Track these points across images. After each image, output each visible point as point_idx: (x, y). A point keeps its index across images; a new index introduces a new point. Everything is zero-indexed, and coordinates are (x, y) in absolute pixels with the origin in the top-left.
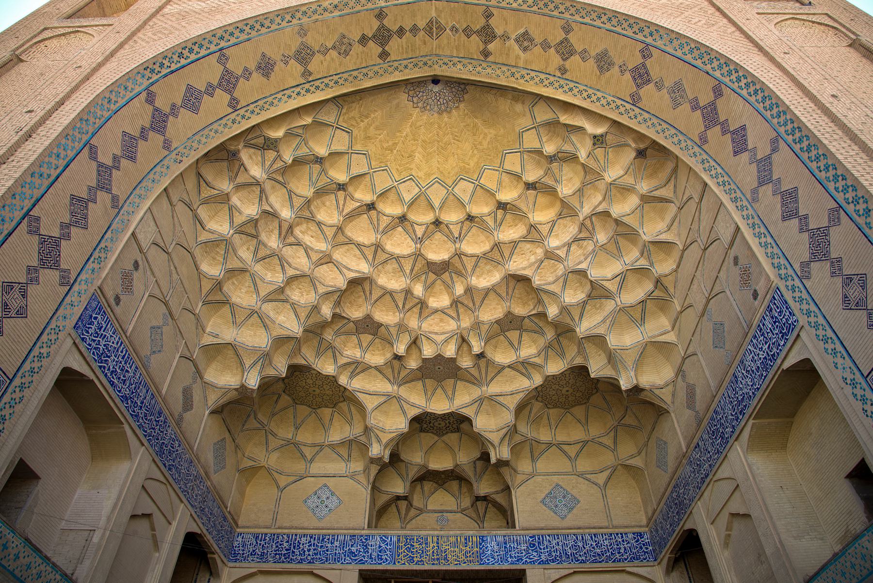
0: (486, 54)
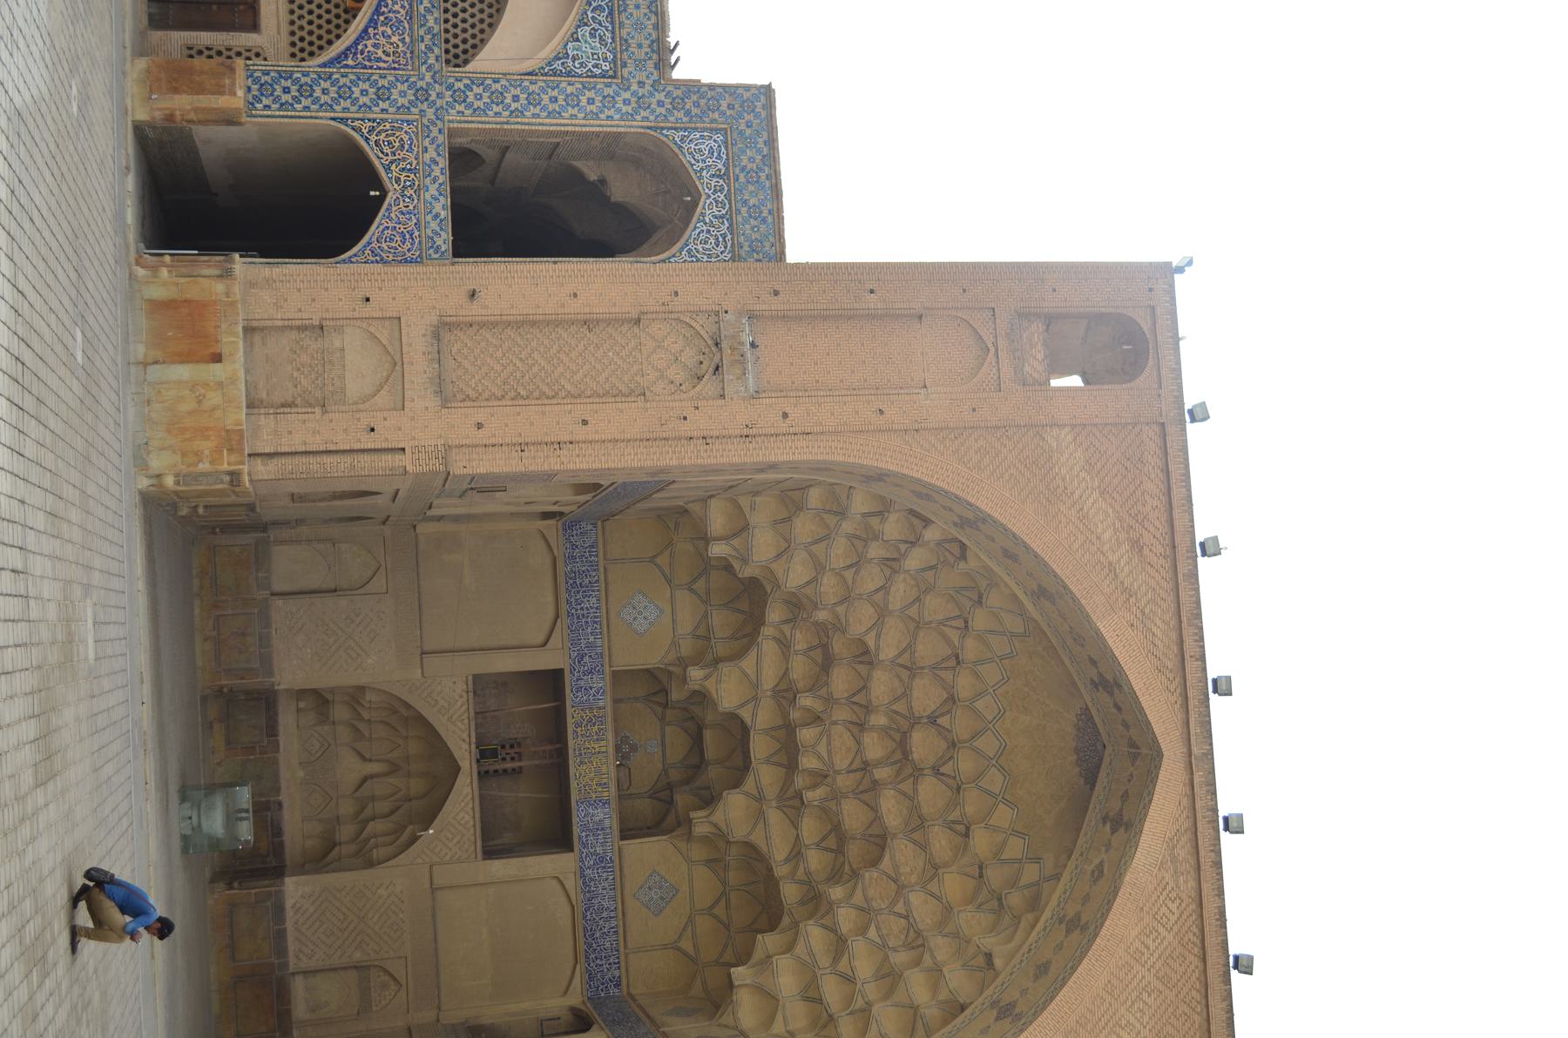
0: (1104, 820)
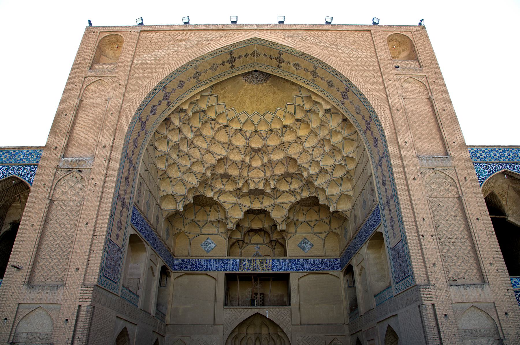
0: (280, 67)
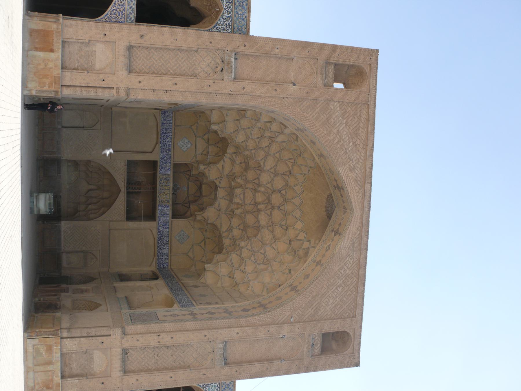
0: (332, 231)
